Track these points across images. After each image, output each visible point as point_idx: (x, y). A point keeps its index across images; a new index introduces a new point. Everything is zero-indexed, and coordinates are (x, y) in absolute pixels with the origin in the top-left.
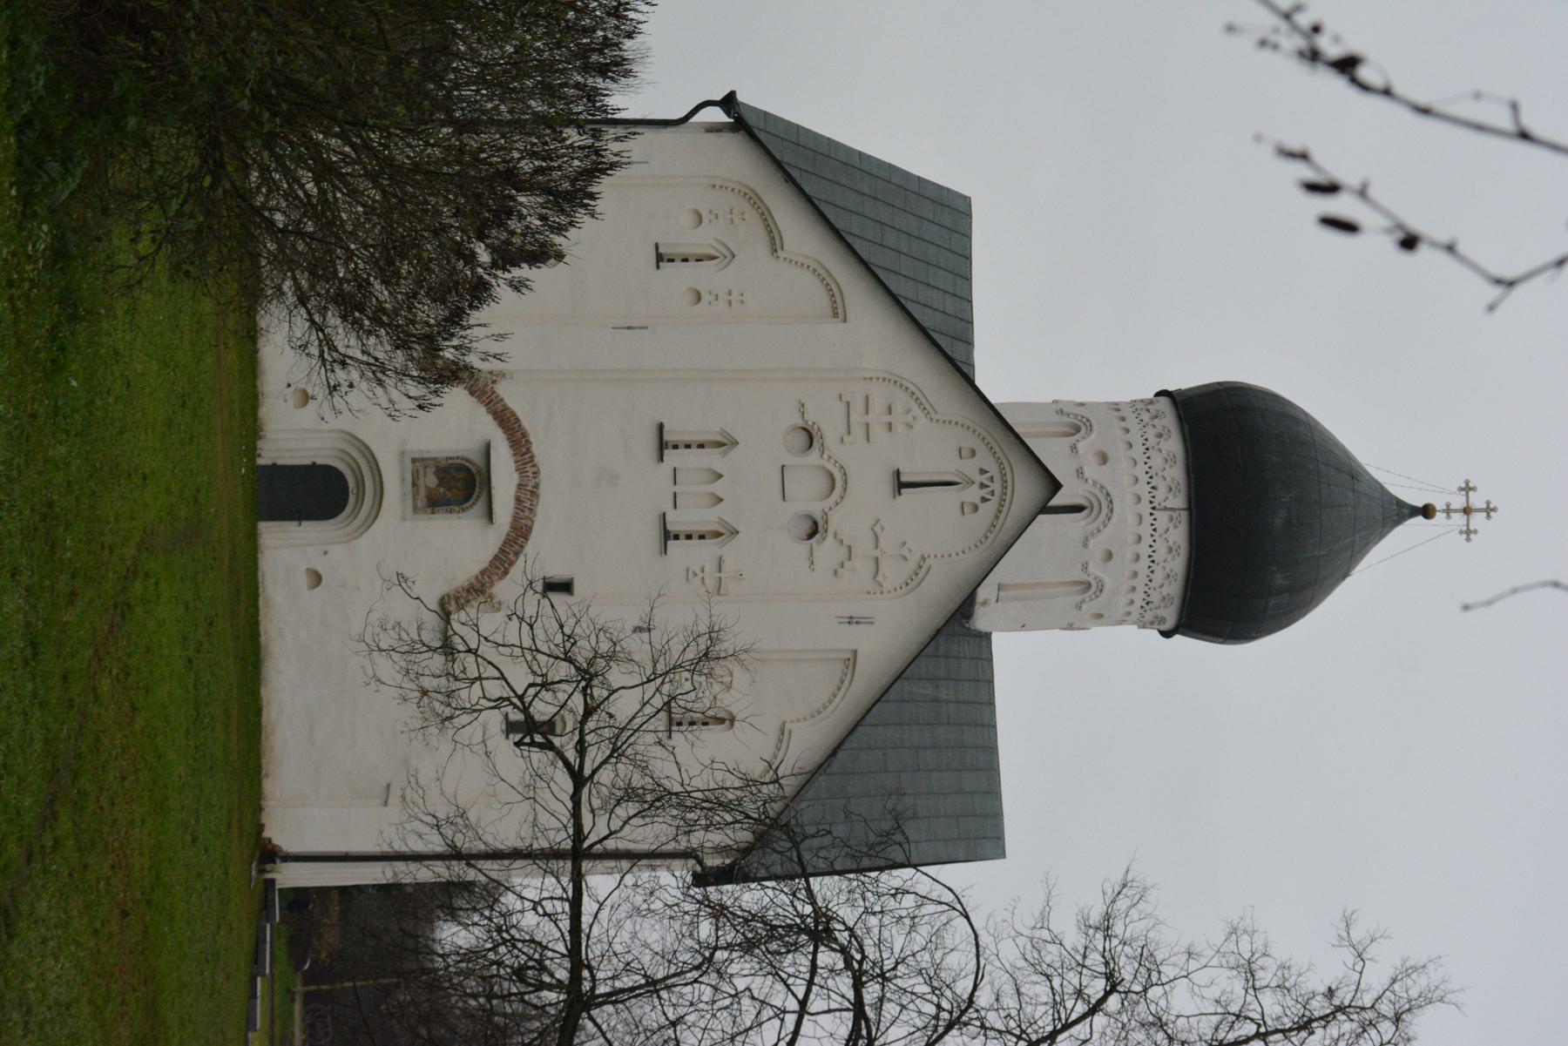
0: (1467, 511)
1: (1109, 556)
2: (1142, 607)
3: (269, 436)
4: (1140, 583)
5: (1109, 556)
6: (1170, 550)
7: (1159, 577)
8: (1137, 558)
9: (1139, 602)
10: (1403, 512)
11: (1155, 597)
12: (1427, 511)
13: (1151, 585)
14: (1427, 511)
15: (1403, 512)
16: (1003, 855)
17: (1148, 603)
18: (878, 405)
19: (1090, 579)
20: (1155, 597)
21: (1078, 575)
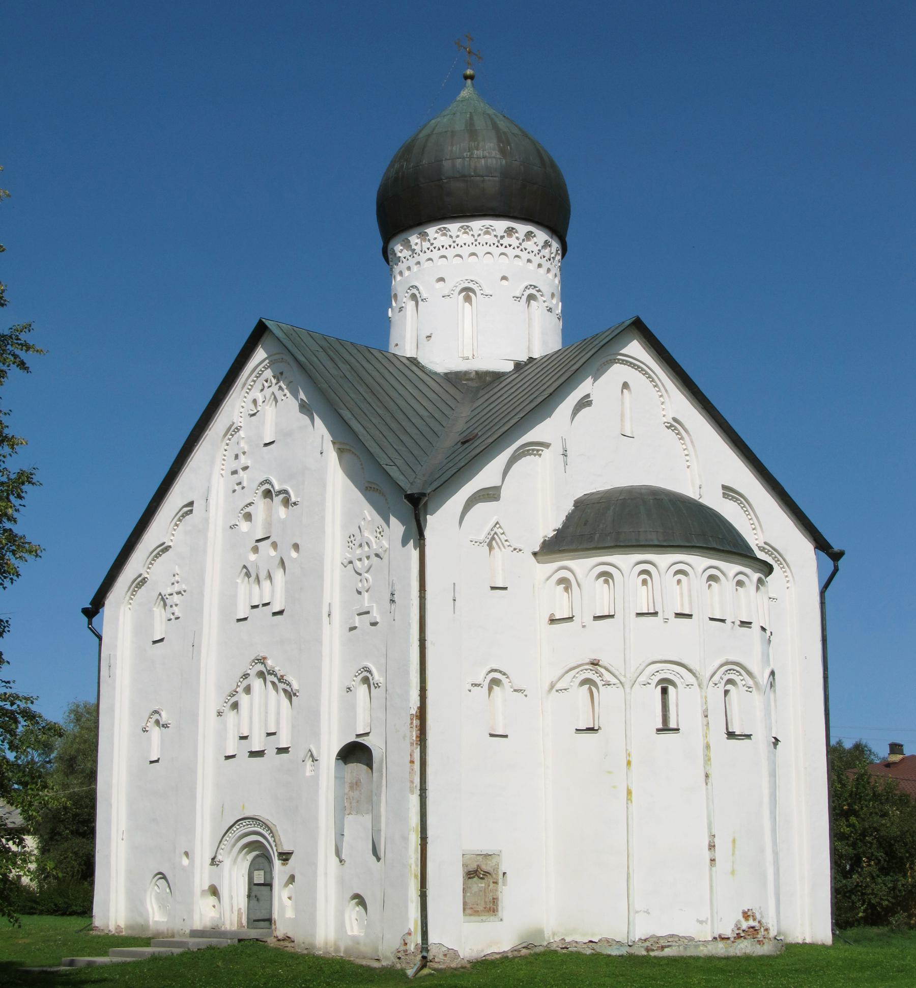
18: (235, 465)
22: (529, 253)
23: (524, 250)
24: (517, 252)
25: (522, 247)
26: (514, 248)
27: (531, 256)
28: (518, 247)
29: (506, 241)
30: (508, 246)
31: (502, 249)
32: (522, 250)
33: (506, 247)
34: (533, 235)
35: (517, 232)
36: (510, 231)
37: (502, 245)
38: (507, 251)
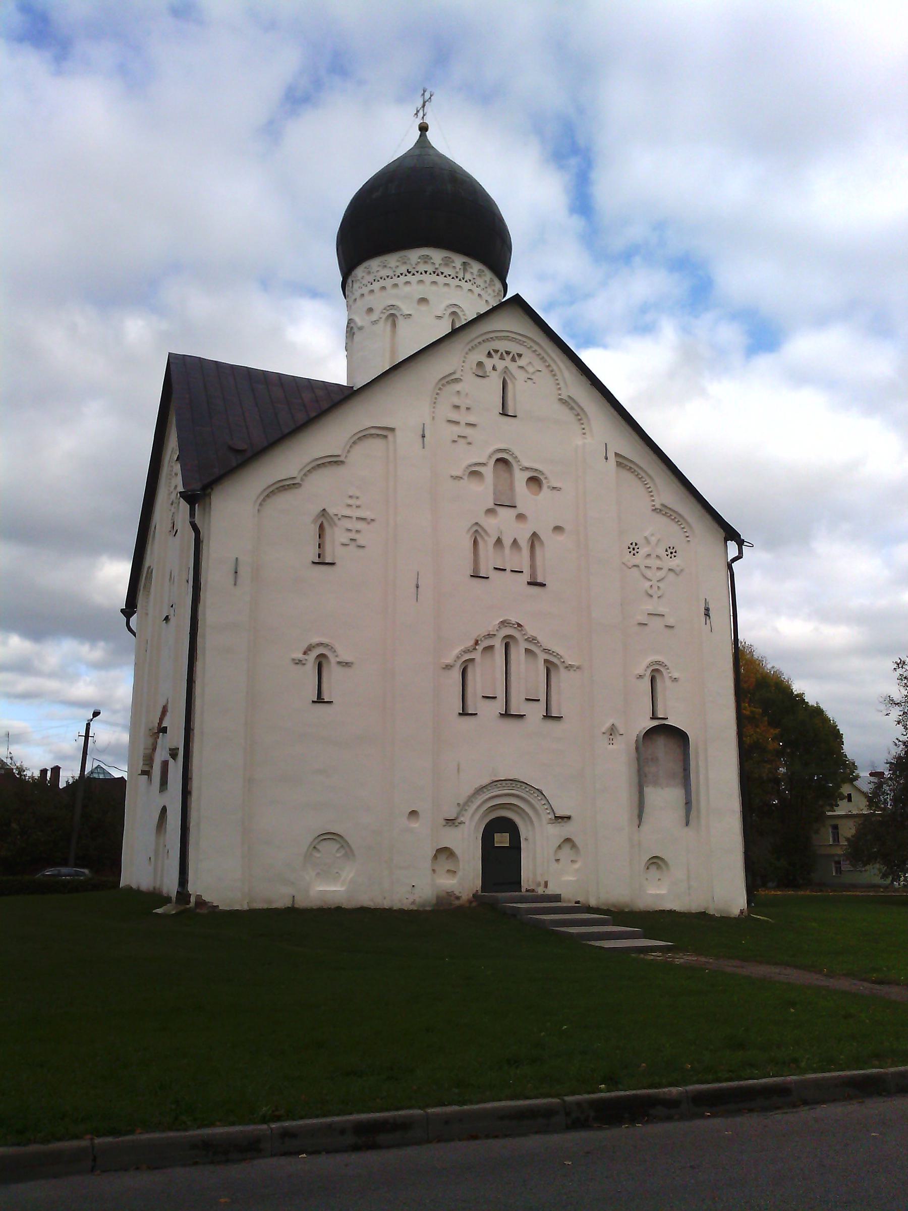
0: (424, 106)
1: (370, 310)
2: (414, 275)
3: (158, 886)
4: (388, 283)
5: (370, 310)
6: (369, 273)
7: (384, 273)
8: (372, 291)
9: (409, 277)
10: (423, 141)
11: (403, 269)
12: (423, 128)
13: (391, 274)
14: (423, 128)
15: (423, 141)
16: (518, 294)
17: (409, 272)
19: (384, 316)
20: (403, 269)
21: (384, 328)
22: (445, 277)
23: (440, 274)
24: (434, 278)
25: (438, 271)
26: (430, 274)
27: (448, 280)
28: (434, 272)
29: (422, 268)
30: (423, 273)
31: (418, 277)
32: (438, 275)
33: (421, 274)
34: (451, 260)
35: (431, 258)
36: (426, 259)
37: (417, 272)
38: (424, 277)
